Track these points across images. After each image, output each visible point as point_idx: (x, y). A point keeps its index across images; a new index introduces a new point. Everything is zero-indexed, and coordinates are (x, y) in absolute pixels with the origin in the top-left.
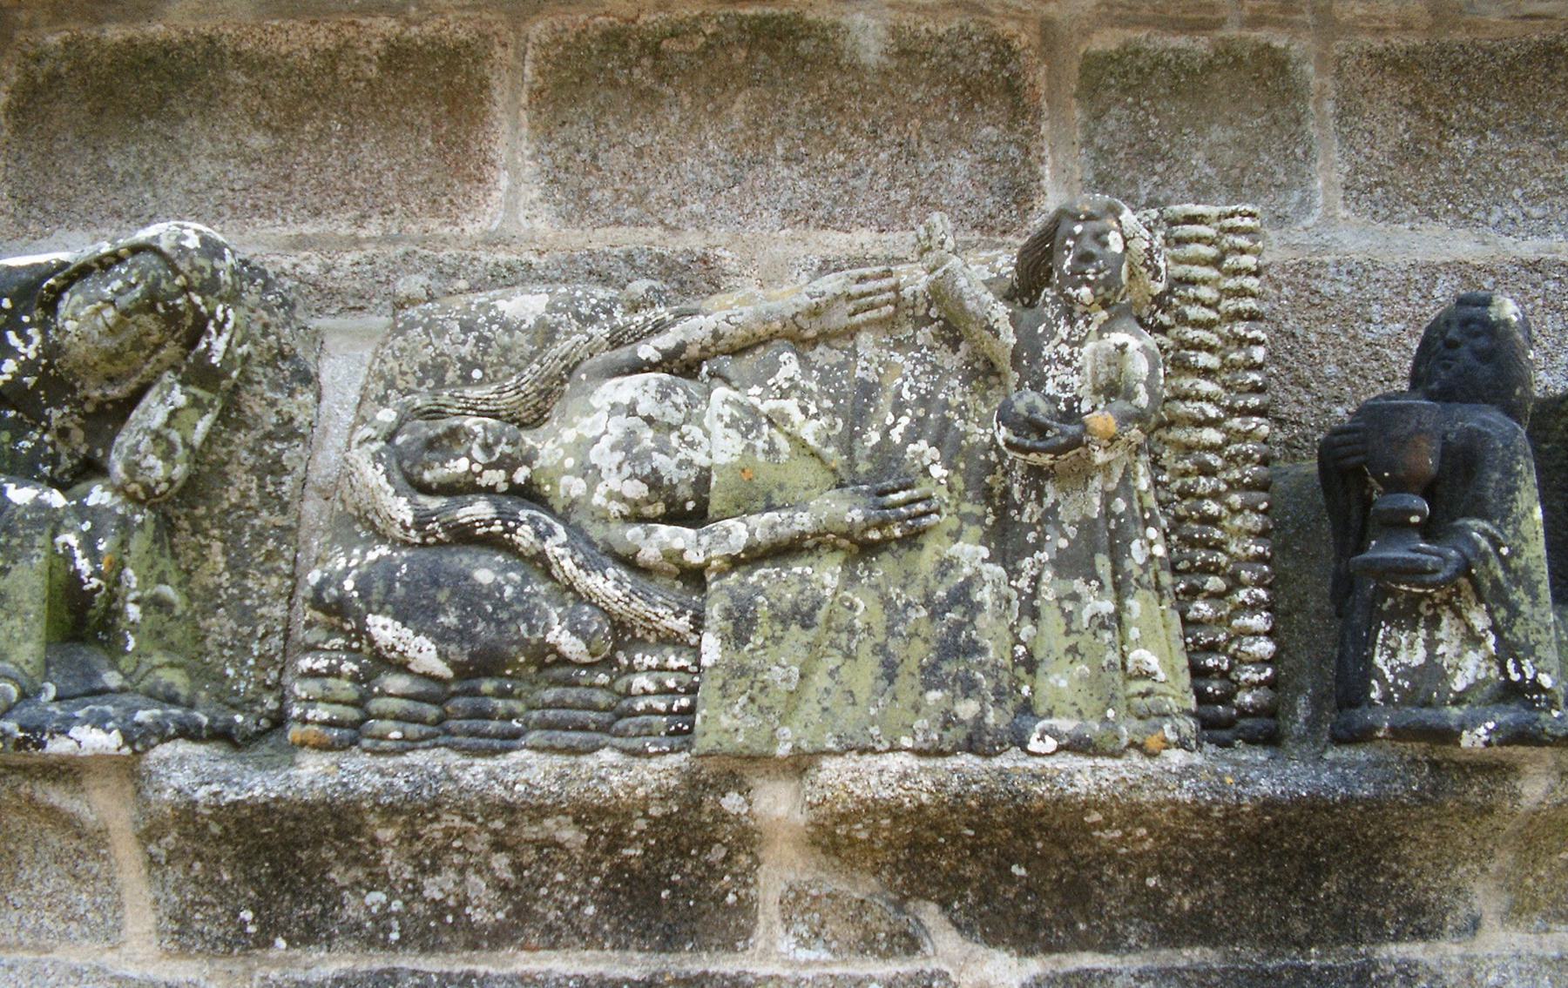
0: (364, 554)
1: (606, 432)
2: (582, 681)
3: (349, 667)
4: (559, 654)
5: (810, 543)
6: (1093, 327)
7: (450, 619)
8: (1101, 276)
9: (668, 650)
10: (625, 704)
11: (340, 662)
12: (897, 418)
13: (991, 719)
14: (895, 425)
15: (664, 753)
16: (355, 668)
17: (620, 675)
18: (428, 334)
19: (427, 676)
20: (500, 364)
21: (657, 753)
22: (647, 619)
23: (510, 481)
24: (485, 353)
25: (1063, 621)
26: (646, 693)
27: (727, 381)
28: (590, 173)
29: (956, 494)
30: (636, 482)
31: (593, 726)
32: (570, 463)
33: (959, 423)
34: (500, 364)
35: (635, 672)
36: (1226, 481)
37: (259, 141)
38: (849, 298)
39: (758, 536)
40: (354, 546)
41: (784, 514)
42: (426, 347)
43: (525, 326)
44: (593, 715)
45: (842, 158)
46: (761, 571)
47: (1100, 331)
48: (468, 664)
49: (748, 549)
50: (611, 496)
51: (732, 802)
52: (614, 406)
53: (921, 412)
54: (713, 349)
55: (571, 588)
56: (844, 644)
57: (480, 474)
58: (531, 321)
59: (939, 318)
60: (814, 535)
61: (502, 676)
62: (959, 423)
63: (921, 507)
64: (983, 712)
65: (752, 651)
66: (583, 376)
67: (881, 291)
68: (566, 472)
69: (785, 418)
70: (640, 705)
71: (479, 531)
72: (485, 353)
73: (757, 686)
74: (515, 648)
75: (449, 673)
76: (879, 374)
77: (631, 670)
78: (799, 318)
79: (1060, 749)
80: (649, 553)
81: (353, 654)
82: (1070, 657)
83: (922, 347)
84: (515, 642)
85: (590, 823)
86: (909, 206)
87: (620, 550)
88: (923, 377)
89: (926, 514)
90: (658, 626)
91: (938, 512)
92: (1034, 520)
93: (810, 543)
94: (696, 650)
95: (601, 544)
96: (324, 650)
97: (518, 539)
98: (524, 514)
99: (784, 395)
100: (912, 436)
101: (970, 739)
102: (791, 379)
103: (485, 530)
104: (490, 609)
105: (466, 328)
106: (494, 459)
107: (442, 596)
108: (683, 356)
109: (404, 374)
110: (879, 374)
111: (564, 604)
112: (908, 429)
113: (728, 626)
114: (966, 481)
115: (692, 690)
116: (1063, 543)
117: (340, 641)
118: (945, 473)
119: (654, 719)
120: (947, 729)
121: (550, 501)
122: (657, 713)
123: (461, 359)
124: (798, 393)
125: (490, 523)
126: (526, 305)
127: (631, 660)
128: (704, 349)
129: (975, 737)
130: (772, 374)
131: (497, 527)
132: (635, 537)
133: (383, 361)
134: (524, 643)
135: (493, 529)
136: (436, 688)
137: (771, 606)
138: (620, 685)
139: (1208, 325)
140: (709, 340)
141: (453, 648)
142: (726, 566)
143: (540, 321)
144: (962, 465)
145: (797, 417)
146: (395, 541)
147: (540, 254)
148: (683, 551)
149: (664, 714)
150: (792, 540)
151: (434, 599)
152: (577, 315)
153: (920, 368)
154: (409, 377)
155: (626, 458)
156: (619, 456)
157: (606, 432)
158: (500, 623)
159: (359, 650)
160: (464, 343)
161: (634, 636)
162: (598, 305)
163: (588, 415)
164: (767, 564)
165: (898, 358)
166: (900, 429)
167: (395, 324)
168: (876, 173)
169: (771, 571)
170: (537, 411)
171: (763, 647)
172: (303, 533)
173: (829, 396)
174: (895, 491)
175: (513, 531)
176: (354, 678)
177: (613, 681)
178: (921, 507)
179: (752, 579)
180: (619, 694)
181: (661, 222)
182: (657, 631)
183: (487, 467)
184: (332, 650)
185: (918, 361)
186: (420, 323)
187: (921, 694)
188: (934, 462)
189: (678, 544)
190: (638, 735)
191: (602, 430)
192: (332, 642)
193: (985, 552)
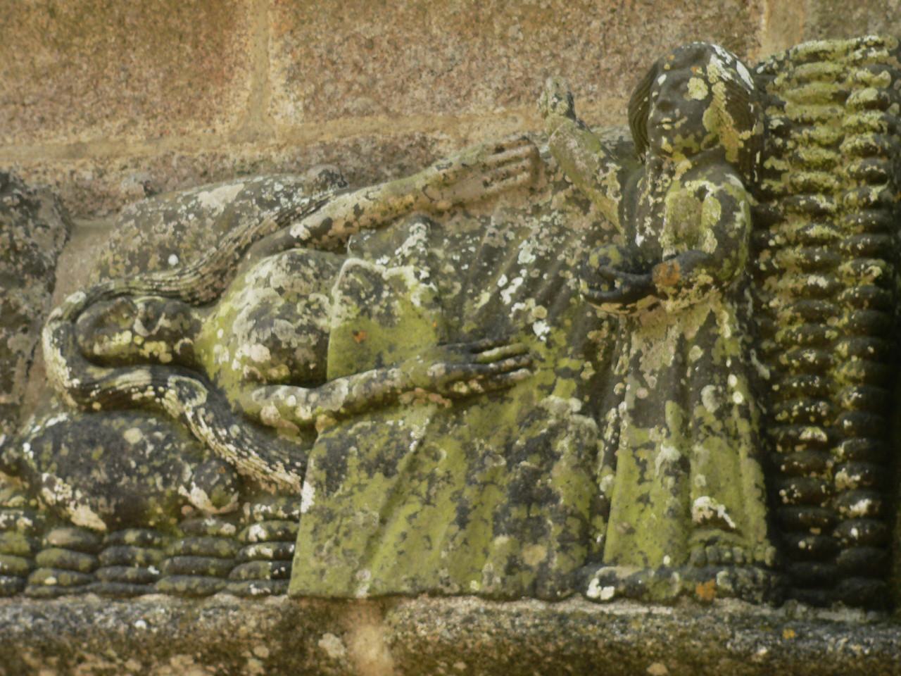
2: (210, 531)
3: (25, 522)
6: (677, 177)
7: (100, 475)
8: (678, 125)
11: (17, 517)
12: (510, 279)
13: (556, 563)
14: (506, 286)
22: (265, 472)
23: (173, 353)
25: (637, 470)
28: (325, 67)
31: (212, 571)
36: (836, 329)
37: (45, 57)
38: (485, 168)
43: (215, 214)
44: (213, 561)
45: (556, 30)
47: (683, 179)
48: (116, 515)
49: (347, 404)
51: (330, 644)
54: (356, 224)
57: (142, 346)
58: (222, 209)
63: (510, 362)
64: (549, 557)
70: (251, 551)
72: (180, 240)
73: (343, 530)
75: (101, 526)
78: (429, 190)
79: (617, 597)
80: (269, 412)
82: (641, 505)
84: (152, 494)
85: (209, 663)
86: (619, 73)
89: (515, 369)
92: (623, 372)
95: (233, 405)
99: (405, 261)
100: (523, 295)
101: (534, 585)
104: (133, 464)
106: (154, 332)
108: (330, 233)
109: (115, 262)
112: (519, 289)
113: (323, 476)
114: (570, 339)
116: (643, 393)
119: (261, 564)
122: (265, 558)
125: (143, 389)
128: (348, 224)
129: (539, 582)
131: (150, 393)
134: (159, 495)
135: (146, 394)
137: (360, 455)
138: (242, 537)
139: (827, 166)
140: (351, 217)
141: (102, 501)
143: (229, 208)
144: (568, 322)
150: (385, 395)
153: (546, 231)
154: (120, 266)
155: (255, 326)
158: (140, 476)
160: (165, 231)
166: (512, 289)
168: (587, 43)
171: (351, 493)
172: (22, 411)
174: (490, 348)
175: (161, 395)
178: (510, 362)
181: (386, 110)
183: (148, 339)
188: (539, 320)
190: (246, 579)
193: (576, 405)
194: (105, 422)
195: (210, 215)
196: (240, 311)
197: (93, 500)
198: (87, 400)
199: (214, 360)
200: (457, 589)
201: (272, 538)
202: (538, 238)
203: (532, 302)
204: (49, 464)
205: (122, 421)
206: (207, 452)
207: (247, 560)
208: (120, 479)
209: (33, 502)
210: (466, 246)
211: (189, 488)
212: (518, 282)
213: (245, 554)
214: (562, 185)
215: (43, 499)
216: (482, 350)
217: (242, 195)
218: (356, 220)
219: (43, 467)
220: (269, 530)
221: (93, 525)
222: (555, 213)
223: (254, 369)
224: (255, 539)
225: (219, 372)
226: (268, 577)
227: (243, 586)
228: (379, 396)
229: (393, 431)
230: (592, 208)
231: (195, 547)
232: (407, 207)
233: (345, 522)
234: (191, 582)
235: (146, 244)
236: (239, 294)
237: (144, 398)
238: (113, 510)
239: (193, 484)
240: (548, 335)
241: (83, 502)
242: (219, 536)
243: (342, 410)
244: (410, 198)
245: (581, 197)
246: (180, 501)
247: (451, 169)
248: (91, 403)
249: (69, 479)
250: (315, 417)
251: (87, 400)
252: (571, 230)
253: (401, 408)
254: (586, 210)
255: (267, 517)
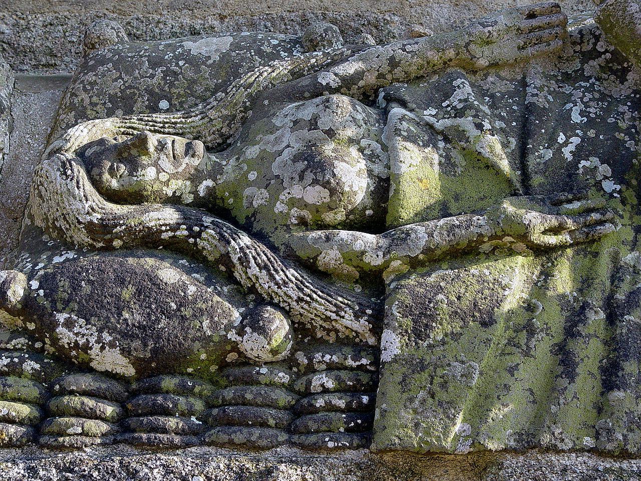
0: (50, 259)
1: (288, 146)
2: (261, 378)
3: (31, 366)
4: (240, 353)
5: (486, 247)
7: (133, 316)
9: (347, 350)
10: (305, 401)
11: (22, 360)
12: (568, 138)
14: (566, 144)
15: (344, 448)
16: (37, 366)
17: (298, 375)
18: (118, 70)
19: (109, 375)
20: (187, 95)
21: (336, 448)
22: (328, 319)
23: (195, 193)
24: (172, 85)
26: (326, 391)
27: (403, 104)
29: (628, 207)
30: (318, 188)
31: (272, 422)
32: (252, 176)
33: (630, 144)
34: (187, 95)
35: (315, 371)
39: (437, 238)
40: (41, 252)
41: (462, 218)
42: (116, 80)
44: (273, 412)
46: (441, 273)
48: (151, 360)
49: (427, 251)
50: (292, 203)
52: (295, 122)
53: (591, 133)
54: (389, 77)
55: (252, 290)
56: (523, 342)
57: (167, 183)
59: (607, 51)
60: (491, 238)
61: (182, 374)
62: (630, 144)
63: (595, 216)
65: (430, 346)
66: (266, 102)
67: (550, 26)
68: (250, 184)
69: (461, 135)
70: (320, 402)
71: (165, 236)
72: (172, 85)
73: (437, 380)
74: (197, 344)
75: (131, 371)
76: (548, 102)
77: (311, 369)
78: (472, 47)
80: (330, 257)
81: (37, 355)
83: (590, 77)
87: (302, 254)
88: (591, 103)
89: (601, 223)
90: (338, 326)
91: (612, 221)
93: (486, 247)
94: (376, 351)
95: (282, 248)
96: (7, 350)
97: (201, 244)
98: (207, 220)
99: (459, 113)
102: (466, 100)
103: (170, 234)
104: (174, 306)
105: (154, 64)
106: (180, 170)
107: (127, 293)
110: (548, 102)
111: (245, 305)
113: (408, 322)
115: (372, 389)
117: (22, 340)
118: (618, 187)
120: (632, 430)
121: (233, 213)
123: (150, 92)
124: (473, 112)
125: (175, 228)
126: (210, 47)
127: (310, 360)
128: (381, 76)
130: (447, 96)
131: (183, 232)
132: (316, 240)
133: (74, 95)
135: (178, 233)
136: (118, 387)
137: (450, 303)
138: (300, 386)
140: (386, 68)
141: (137, 344)
142: (406, 268)
143: (224, 56)
144: (634, 182)
145: (473, 132)
146: (81, 246)
147: (222, 18)
148: (363, 253)
149: (342, 411)
151: (119, 298)
152: (260, 53)
153: (588, 96)
156: (301, 165)
157: (288, 146)
158: (183, 318)
159: (43, 349)
160: (152, 76)
161: (314, 338)
162: (279, 45)
163: (271, 133)
164: (445, 266)
165: (567, 89)
166: (571, 147)
167: (86, 63)
169: (450, 272)
170: (221, 135)
171: (443, 343)
173: (502, 118)
174: (569, 201)
175: (198, 235)
176: (36, 377)
177: (292, 381)
178: (595, 216)
179: (432, 279)
180: (298, 393)
182: (337, 331)
183: (174, 176)
184: (15, 349)
185: (587, 90)
186: (110, 60)
187: (602, 394)
188: (606, 178)
189: (358, 246)
190: (317, 432)
191: (284, 145)
192: (14, 342)
194: (131, 260)
195: (204, 63)
196: (280, 153)
197: (125, 344)
198: (109, 236)
199: (245, 203)
200: (570, 445)
201: (341, 390)
202: (582, 101)
203: (595, 161)
204: (66, 303)
205: (150, 262)
206: (252, 297)
207: (316, 411)
208: (158, 320)
209: (38, 345)
210: (510, 106)
211: (241, 332)
212: (576, 140)
213: (312, 405)
214: (594, 54)
215: (55, 341)
216: (561, 203)
217: (235, 46)
218: (390, 72)
219: (60, 306)
220: (338, 379)
221: (119, 370)
222: (593, 80)
223: (305, 213)
224: (320, 389)
225: (254, 215)
226: (342, 430)
227: (313, 439)
228: (464, 244)
229: (481, 280)
230: (630, 76)
231: (249, 396)
232: (445, 63)
233: (440, 372)
234: (251, 434)
235: (130, 87)
236: (272, 137)
237: (174, 237)
238: (148, 355)
239: (248, 329)
240: (620, 192)
241: (112, 345)
242: (271, 384)
243: (421, 257)
244: (451, 53)
245: (616, 67)
246: (229, 348)
247: (496, 28)
248: (111, 240)
249: (93, 320)
250: (386, 265)
251: (109, 236)
252: (611, 96)
253: (483, 257)
254: (623, 80)
255: (331, 368)
